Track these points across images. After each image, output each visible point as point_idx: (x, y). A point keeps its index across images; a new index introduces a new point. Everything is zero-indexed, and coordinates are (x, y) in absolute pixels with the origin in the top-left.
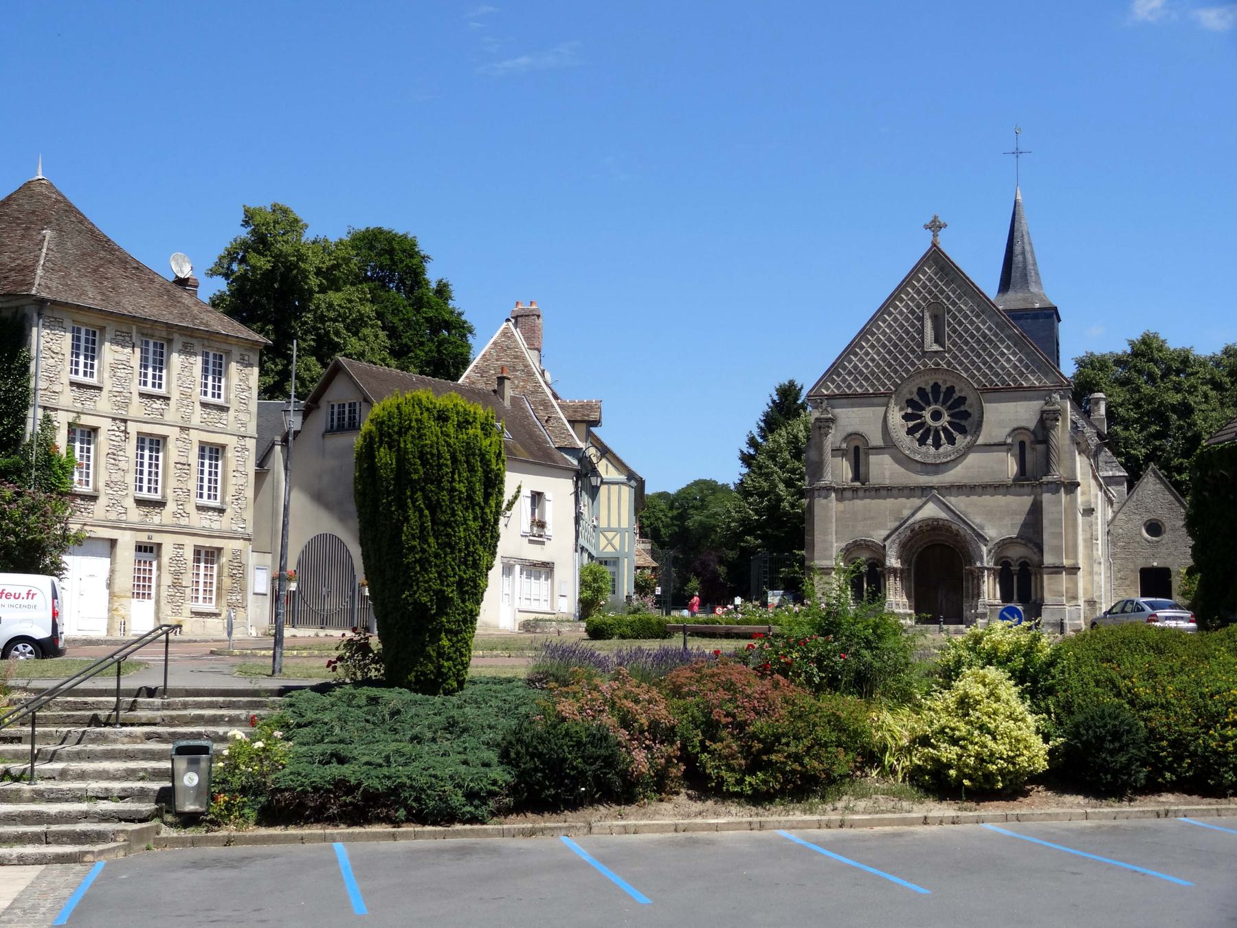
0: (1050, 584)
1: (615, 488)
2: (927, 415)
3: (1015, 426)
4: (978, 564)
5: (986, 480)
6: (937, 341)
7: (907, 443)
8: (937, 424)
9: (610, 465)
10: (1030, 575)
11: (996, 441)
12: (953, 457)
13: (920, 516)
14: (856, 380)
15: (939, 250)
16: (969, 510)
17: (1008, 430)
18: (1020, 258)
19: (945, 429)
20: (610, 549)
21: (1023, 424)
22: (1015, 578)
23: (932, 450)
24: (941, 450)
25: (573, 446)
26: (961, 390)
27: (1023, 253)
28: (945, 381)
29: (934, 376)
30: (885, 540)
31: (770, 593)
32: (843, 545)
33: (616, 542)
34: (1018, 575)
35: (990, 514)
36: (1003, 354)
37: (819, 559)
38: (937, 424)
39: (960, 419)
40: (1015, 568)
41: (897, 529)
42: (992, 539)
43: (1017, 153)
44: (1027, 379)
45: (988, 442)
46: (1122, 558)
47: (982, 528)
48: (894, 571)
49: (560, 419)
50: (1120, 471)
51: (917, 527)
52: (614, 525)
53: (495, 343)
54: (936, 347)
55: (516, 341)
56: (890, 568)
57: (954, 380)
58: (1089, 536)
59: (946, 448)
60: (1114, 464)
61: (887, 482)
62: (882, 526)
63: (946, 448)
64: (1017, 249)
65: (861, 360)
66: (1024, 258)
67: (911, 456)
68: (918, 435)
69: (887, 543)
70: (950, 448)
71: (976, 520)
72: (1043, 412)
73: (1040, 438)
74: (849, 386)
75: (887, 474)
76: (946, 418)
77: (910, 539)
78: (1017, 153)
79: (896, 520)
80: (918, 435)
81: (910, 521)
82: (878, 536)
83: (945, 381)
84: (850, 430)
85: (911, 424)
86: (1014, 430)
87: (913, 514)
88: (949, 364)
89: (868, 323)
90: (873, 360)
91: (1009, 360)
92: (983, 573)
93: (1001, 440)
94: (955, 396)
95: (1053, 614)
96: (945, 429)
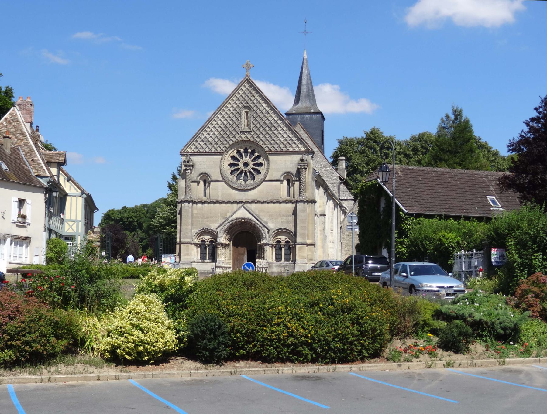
0: (299, 253)
1: (74, 198)
3: (285, 171)
4: (264, 242)
5: (270, 199)
6: (247, 126)
7: (232, 178)
9: (72, 187)
12: (253, 186)
13: (236, 216)
14: (206, 145)
15: (250, 79)
16: (261, 214)
17: (281, 173)
19: (250, 172)
20: (70, 231)
21: (289, 170)
23: (243, 183)
24: (248, 183)
25: (45, 175)
29: (245, 144)
30: (217, 228)
31: (163, 256)
32: (195, 231)
33: (74, 227)
35: (271, 216)
37: (184, 238)
38: (246, 169)
39: (258, 166)
41: (223, 223)
42: (273, 229)
43: (305, 33)
44: (292, 147)
45: (271, 179)
46: (347, 240)
47: (267, 223)
49: (39, 160)
50: (350, 196)
52: (73, 218)
53: (6, 119)
54: (247, 129)
55: (18, 118)
56: (219, 244)
59: (250, 181)
60: (347, 193)
61: (220, 199)
62: (216, 221)
63: (250, 181)
67: (232, 185)
69: (218, 230)
70: (252, 182)
71: (264, 219)
72: (299, 164)
74: (202, 147)
75: (220, 195)
76: (251, 166)
78: (305, 33)
79: (224, 218)
81: (230, 219)
82: (213, 226)
84: (202, 171)
87: (232, 215)
93: (278, 178)
96: (250, 172)
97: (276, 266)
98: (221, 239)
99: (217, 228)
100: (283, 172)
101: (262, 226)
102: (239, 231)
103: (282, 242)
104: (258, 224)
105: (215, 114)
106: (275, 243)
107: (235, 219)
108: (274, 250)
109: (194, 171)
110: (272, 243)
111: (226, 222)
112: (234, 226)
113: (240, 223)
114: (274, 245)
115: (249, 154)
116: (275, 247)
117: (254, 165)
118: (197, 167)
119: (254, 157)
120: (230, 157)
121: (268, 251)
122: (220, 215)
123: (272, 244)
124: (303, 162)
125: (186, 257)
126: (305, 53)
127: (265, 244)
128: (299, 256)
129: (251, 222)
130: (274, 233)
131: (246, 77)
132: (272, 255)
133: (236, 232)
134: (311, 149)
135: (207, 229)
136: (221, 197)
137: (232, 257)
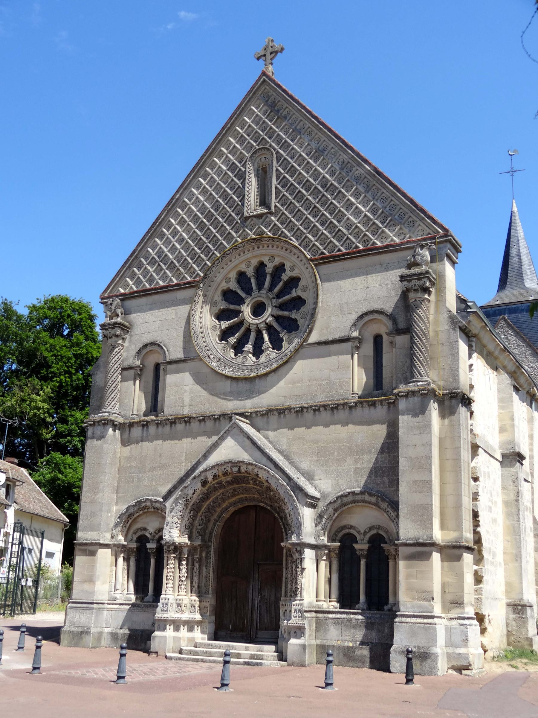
0: (408, 576)
2: (246, 310)
3: (365, 310)
5: (321, 399)
8: (259, 321)
10: (387, 558)
11: (336, 336)
12: (274, 366)
17: (354, 317)
18: (516, 259)
22: (363, 562)
26: (292, 268)
27: (519, 255)
28: (272, 258)
30: (166, 497)
32: (123, 508)
34: (367, 557)
36: (349, 205)
37: (85, 529)
40: (362, 546)
43: (512, 172)
45: (323, 339)
48: (177, 549)
51: (210, 476)
57: (282, 253)
58: (512, 497)
61: (186, 411)
64: (513, 252)
65: (167, 242)
66: (520, 259)
68: (233, 340)
73: (402, 325)
75: (187, 400)
77: (205, 497)
80: (233, 340)
83: (272, 258)
85: (225, 324)
86: (362, 316)
87: (206, 456)
88: (275, 230)
89: (178, 191)
90: (181, 240)
91: (357, 213)
92: (301, 553)
94: (285, 277)
95: (413, 634)
96: (269, 328)
97: (337, 622)
99: (166, 497)
100: (359, 314)
103: (358, 538)
105: (184, 187)
109: (130, 341)
112: (215, 489)
113: (229, 478)
115: (268, 279)
117: (281, 307)
118: (137, 330)
119: (281, 284)
120: (219, 293)
122: (183, 459)
124: (414, 270)
125: (86, 586)
126: (514, 205)
128: (410, 589)
131: (260, 78)
133: (227, 508)
134: (445, 230)
135: (151, 501)
136: (190, 405)
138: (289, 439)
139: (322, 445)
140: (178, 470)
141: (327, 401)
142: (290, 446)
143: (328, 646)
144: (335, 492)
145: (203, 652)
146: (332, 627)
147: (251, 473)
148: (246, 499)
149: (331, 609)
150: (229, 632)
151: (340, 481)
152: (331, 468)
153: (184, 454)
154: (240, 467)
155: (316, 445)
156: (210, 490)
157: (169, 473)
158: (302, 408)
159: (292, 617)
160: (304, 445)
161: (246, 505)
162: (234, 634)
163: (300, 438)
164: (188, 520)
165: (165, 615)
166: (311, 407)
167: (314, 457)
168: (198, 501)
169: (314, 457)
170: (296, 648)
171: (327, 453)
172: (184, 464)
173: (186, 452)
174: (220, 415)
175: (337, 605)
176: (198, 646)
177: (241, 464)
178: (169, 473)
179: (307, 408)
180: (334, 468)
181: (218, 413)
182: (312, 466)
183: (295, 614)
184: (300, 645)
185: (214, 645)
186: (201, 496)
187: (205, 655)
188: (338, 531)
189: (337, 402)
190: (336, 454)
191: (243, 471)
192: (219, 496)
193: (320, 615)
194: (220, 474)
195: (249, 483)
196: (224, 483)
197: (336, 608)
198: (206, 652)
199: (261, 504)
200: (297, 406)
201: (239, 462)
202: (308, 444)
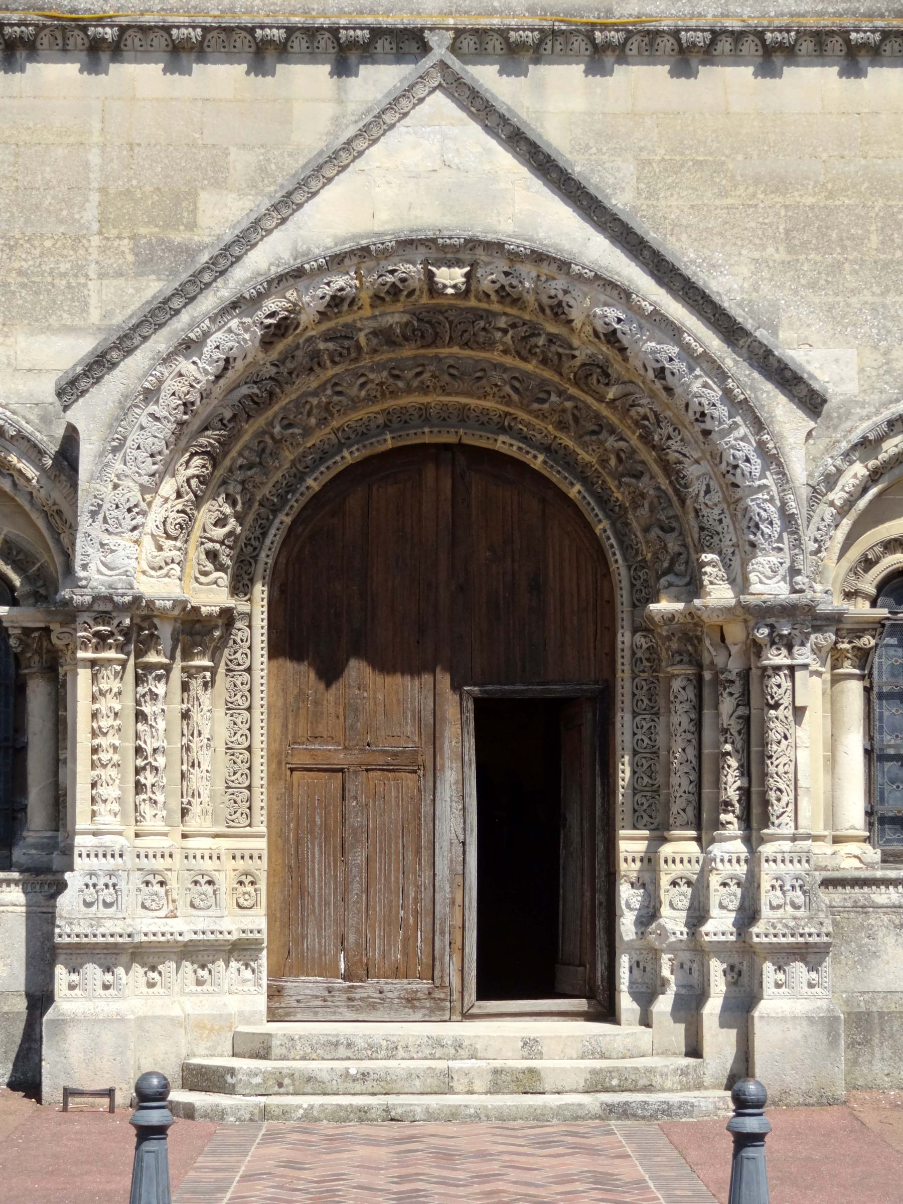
42: (848, 404)
98: (123, 544)
101: (729, 359)
102: (363, 434)
104: (674, 332)
106: (862, 608)
107: (337, 261)
108: (854, 691)
110: (835, 603)
111: (208, 303)
112: (315, 361)
114: (859, 629)
116: (863, 657)
121: (815, 717)
122: (90, 214)
123: (834, 620)
127: (788, 611)
129: (558, 311)
130: (859, 470)
132: (832, 762)
133: (323, 455)
137: (260, 798)
138: (650, 162)
139: (809, 200)
140: (64, 267)
141: (821, 14)
142: (652, 194)
143: (881, 1015)
144: (876, 397)
145: (346, 1075)
146: (890, 940)
147: (530, 298)
148: (424, 415)
149: (849, 866)
150: (340, 983)
151: (895, 354)
152: (854, 300)
153: (95, 197)
154: (474, 265)
155: (780, 199)
156: (290, 365)
157: (12, 278)
158: (716, 34)
159: (765, 911)
160: (723, 193)
161: (427, 439)
162: (370, 988)
163: (699, 165)
164: (179, 495)
165: (109, 927)
166: (760, 35)
167: (771, 250)
168: (228, 414)
169: (771, 250)
170: (796, 1033)
171: (834, 235)
172: (96, 241)
173: (103, 190)
174: (291, 30)
175: (873, 854)
176: (276, 1051)
177: (481, 255)
178: (12, 278)
179: (738, 36)
180: (869, 298)
181: (282, 19)
182: (765, 288)
183: (777, 897)
184: (810, 1019)
185: (361, 1043)
186: (245, 390)
187: (358, 1087)
188: (868, 563)
189: (880, 23)
190: (874, 240)
191: (486, 284)
192: (315, 393)
193: (837, 896)
194: (365, 297)
195: (489, 345)
196: (362, 338)
197: (870, 866)
198: (365, 1075)
199: (504, 444)
200: (693, 23)
201: (473, 244)
202: (741, 191)
